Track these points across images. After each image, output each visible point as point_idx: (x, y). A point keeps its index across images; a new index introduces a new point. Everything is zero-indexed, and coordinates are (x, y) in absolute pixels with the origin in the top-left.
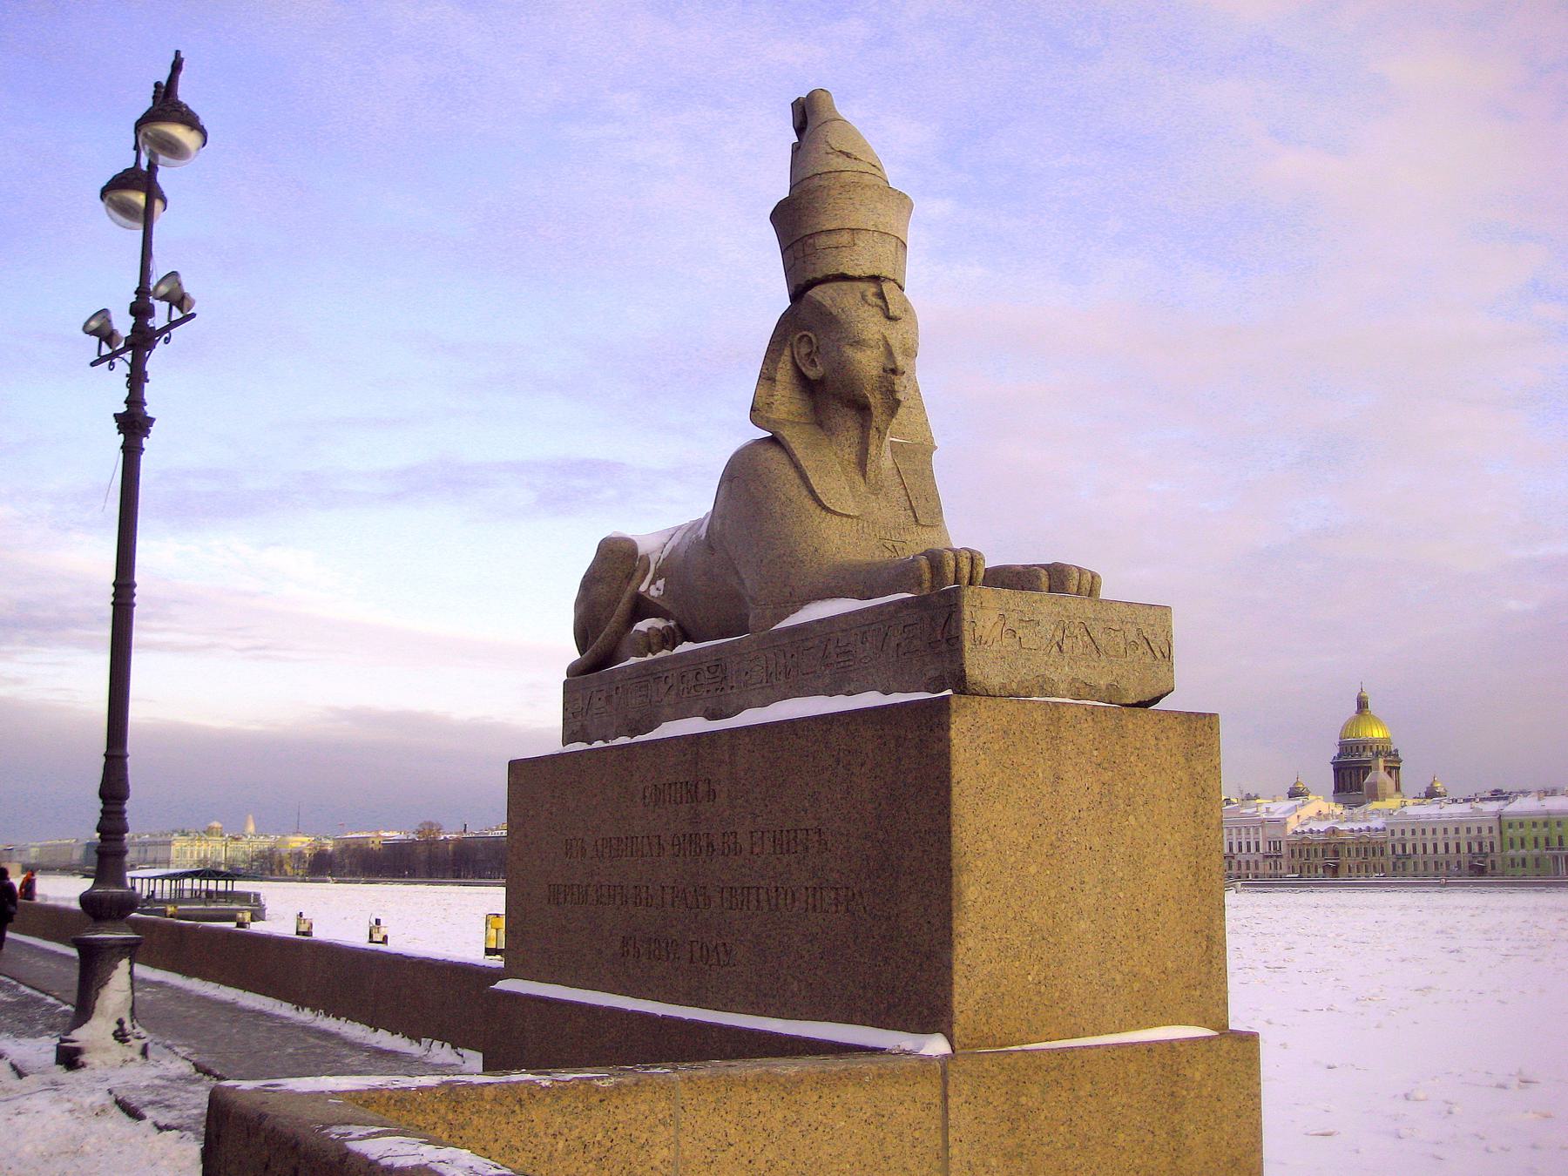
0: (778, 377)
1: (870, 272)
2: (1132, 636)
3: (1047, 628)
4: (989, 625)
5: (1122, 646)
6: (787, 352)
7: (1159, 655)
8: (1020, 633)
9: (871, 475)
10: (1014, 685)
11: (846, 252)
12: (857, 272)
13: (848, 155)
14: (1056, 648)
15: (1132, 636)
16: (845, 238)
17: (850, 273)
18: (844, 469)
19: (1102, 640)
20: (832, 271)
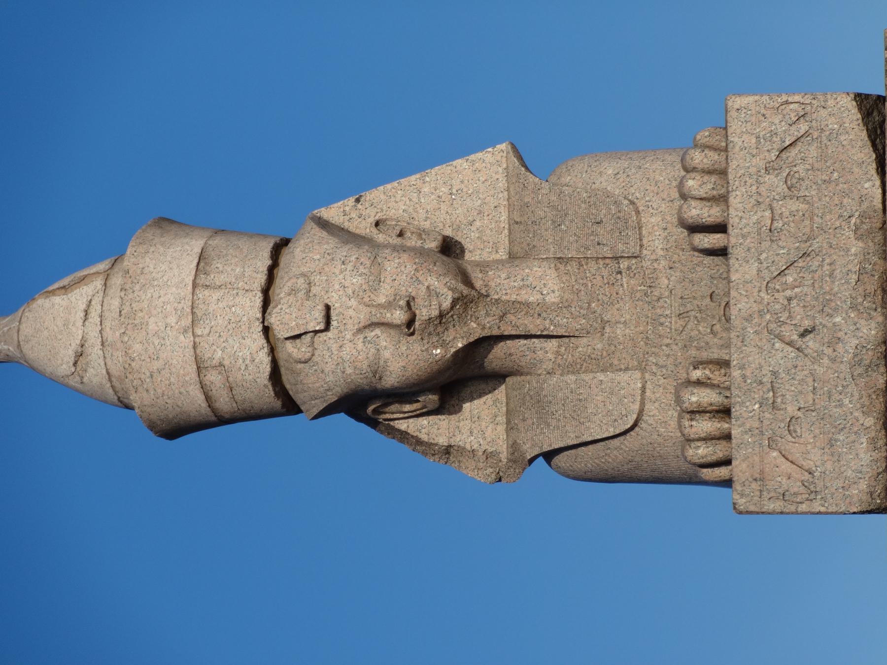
0: (442, 441)
1: (262, 341)
2: (775, 182)
3: (782, 356)
4: (786, 466)
5: (794, 205)
6: (402, 425)
7: (803, 127)
8: (791, 410)
9: (575, 326)
10: (869, 421)
11: (236, 376)
12: (264, 359)
13: (79, 355)
14: (811, 342)
15: (775, 182)
16: (213, 378)
17: (268, 369)
18: (573, 368)
19: (786, 249)
20: (270, 392)
